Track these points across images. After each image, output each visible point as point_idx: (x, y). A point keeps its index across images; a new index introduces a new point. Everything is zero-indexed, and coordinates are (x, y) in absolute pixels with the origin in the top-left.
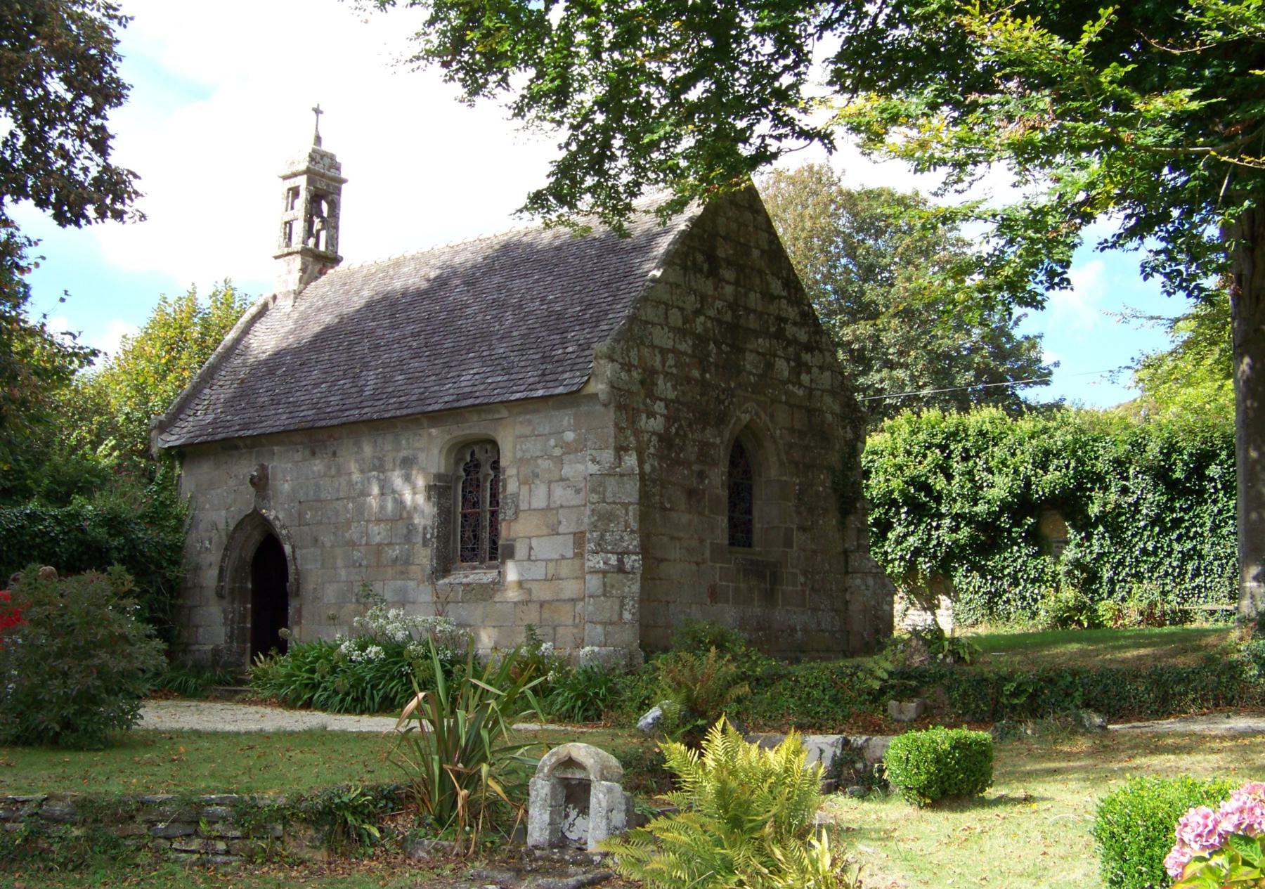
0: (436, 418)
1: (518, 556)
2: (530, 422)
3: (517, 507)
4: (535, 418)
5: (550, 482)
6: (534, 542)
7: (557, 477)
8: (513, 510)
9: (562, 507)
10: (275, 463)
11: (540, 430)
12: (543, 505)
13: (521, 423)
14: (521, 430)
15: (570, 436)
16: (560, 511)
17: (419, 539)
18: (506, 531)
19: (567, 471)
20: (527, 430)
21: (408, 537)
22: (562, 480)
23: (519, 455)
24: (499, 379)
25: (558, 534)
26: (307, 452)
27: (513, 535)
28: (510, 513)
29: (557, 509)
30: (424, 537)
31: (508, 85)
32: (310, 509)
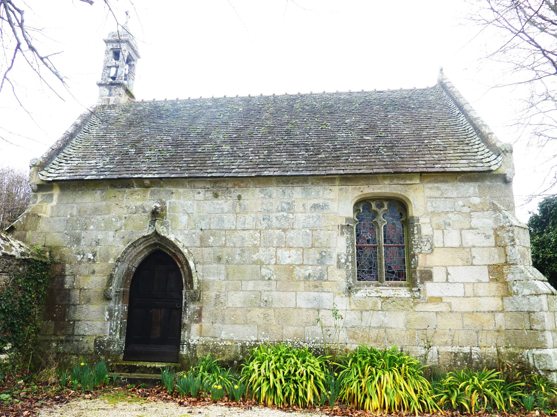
0: (347, 179)
1: (435, 278)
2: (438, 188)
3: (432, 245)
4: (443, 186)
5: (461, 229)
6: (450, 270)
7: (468, 227)
8: (429, 246)
9: (474, 247)
10: (173, 200)
11: (449, 195)
12: (457, 244)
13: (431, 188)
14: (428, 193)
15: (476, 200)
16: (473, 249)
17: (334, 262)
18: (423, 261)
19: (475, 222)
20: (437, 194)
21: (321, 260)
22: (471, 228)
23: (430, 209)
24: (157, 166)
25: (472, 265)
26: (209, 195)
27: (428, 263)
28: (426, 248)
29: (470, 248)
30: (339, 261)
31: (20, 49)
32: (212, 235)
